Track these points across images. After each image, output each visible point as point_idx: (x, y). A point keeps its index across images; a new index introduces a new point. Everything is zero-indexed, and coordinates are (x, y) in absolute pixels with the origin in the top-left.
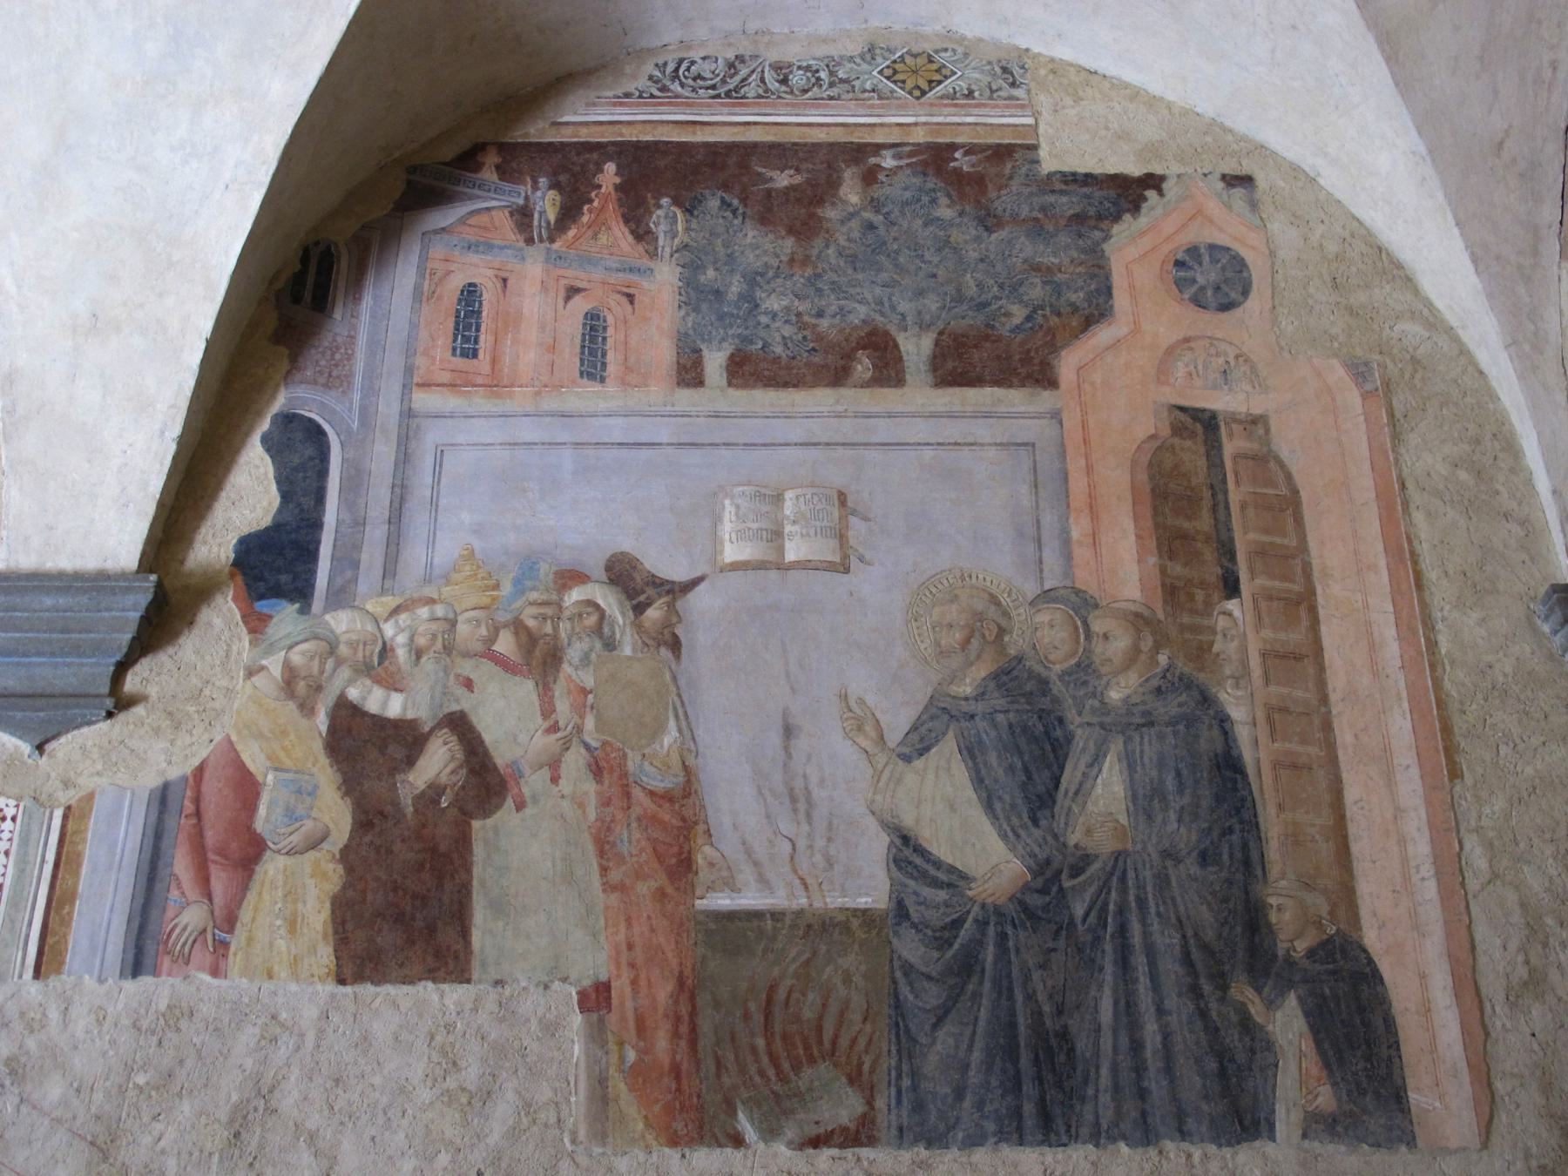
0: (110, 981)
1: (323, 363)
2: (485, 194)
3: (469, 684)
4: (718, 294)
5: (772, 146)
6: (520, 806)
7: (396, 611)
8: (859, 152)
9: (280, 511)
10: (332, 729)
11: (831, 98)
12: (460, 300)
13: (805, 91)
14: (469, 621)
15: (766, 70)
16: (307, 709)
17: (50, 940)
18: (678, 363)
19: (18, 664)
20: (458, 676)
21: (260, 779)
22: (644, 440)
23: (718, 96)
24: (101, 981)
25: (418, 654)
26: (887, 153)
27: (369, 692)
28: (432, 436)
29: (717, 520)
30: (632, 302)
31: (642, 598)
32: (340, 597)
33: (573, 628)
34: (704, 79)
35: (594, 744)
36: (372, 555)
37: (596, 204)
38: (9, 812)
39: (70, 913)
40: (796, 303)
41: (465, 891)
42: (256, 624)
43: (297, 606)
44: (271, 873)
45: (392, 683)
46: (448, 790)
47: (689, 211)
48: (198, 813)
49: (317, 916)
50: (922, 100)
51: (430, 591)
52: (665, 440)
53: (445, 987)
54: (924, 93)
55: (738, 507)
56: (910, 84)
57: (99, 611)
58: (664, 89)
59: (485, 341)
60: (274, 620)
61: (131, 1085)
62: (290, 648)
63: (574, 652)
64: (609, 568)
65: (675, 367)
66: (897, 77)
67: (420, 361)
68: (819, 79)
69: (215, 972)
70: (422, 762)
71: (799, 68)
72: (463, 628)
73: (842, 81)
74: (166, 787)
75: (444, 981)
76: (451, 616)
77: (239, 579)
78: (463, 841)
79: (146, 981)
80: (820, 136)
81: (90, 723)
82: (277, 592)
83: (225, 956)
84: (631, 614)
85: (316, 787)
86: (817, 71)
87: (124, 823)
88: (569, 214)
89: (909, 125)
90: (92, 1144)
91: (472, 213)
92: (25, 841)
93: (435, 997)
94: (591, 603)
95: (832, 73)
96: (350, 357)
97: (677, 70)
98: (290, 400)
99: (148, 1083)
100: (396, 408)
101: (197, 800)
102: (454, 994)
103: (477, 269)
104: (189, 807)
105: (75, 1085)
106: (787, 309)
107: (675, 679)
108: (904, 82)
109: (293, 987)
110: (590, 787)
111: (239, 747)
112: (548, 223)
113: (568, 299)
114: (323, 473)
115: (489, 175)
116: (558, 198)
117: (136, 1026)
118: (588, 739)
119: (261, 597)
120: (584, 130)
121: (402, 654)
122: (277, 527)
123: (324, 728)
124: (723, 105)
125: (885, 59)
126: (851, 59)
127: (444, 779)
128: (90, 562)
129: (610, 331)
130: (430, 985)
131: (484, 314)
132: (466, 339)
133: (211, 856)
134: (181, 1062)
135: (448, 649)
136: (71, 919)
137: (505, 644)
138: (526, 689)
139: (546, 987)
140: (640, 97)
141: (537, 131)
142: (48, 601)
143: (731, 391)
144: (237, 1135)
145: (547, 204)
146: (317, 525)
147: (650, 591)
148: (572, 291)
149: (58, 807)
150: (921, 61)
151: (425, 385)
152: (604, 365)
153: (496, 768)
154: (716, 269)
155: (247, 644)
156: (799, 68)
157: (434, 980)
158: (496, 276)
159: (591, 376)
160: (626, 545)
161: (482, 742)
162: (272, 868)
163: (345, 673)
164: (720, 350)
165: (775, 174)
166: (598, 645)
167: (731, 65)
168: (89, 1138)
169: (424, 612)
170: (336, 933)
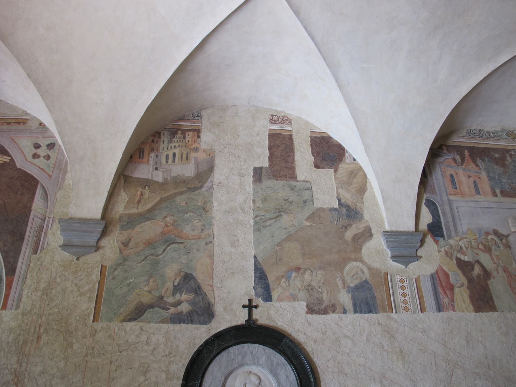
0: (435, 313)
1: (430, 189)
2: (446, 155)
3: (477, 254)
4: (494, 178)
5: (492, 148)
6: (494, 278)
7: (460, 240)
8: (508, 151)
9: (433, 219)
10: (457, 263)
11: (499, 139)
12: (450, 177)
13: (494, 138)
14: (474, 242)
15: (486, 132)
16: (451, 259)
17: (422, 305)
18: (492, 192)
19: (398, 250)
20: (475, 253)
21: (448, 273)
22: (491, 207)
23: (479, 138)
24: (434, 313)
25: (467, 248)
26: (512, 151)
27: (461, 256)
28: (455, 205)
29: (508, 223)
30: (480, 179)
31: (501, 238)
32: (450, 237)
33: (491, 244)
34: (476, 134)
35: (503, 266)
36: (452, 228)
37: (466, 158)
38: (405, 280)
39: (424, 300)
40: (508, 181)
41: (490, 294)
42: (437, 242)
43: (442, 238)
44: (457, 291)
45: (464, 254)
46: (481, 275)
47: (483, 161)
48: (440, 280)
49: (468, 300)
50: (514, 141)
51: (465, 236)
52: (494, 207)
53: (494, 313)
54: (514, 139)
55: (511, 221)
56: (511, 137)
57: (413, 239)
58: (470, 135)
59: (458, 186)
60: (440, 241)
61: (446, 333)
62: (444, 247)
63: (494, 248)
64: (494, 232)
65: (491, 193)
66: (509, 136)
67: (448, 190)
68: (495, 135)
69: (454, 311)
70: (475, 270)
71: (491, 133)
72: (473, 243)
73: (500, 136)
74: (432, 274)
75: (493, 312)
76: (470, 241)
77: (430, 233)
78: (487, 284)
79: (442, 313)
80: (499, 147)
81: (414, 262)
82: (437, 235)
83: (454, 307)
84: (500, 241)
85: (459, 274)
86: (494, 134)
87: (427, 282)
88: (463, 160)
89: (514, 146)
90: (443, 344)
91: (446, 159)
92: (410, 286)
93: (493, 315)
94: (493, 239)
95: (497, 134)
96: (435, 188)
97: (470, 131)
98: (427, 196)
99: (449, 332)
100: (446, 199)
101: (439, 277)
102: (496, 314)
103: (450, 171)
104: (438, 279)
105: (436, 333)
106: (507, 182)
107: (512, 254)
108: (510, 137)
109: (468, 313)
110: (504, 274)
111: (442, 267)
112: (460, 162)
113: (469, 178)
114: (438, 212)
115: (445, 151)
116: (460, 157)
117: (443, 321)
118: (501, 265)
119: (435, 237)
120: (459, 143)
121: (464, 248)
122: (433, 222)
123: (456, 263)
124: (481, 139)
125: (506, 132)
126: (499, 131)
127: (480, 273)
128: (406, 229)
129: (478, 185)
130: (491, 312)
131: (456, 180)
132: (454, 185)
133: (445, 288)
134: (453, 328)
135: (472, 247)
136: (424, 301)
137: (481, 246)
138: (487, 255)
139: (510, 312)
140: (466, 137)
141: (450, 142)
142: (403, 237)
143: (502, 198)
144: (468, 342)
145: (458, 158)
146: (440, 222)
147: (502, 237)
148: (469, 177)
149: (414, 279)
150: (511, 133)
151: (450, 194)
152: (479, 191)
153: (488, 271)
154: (492, 173)
155: (436, 247)
156: (491, 133)
157: (492, 312)
158: (455, 172)
159: (478, 194)
160: (495, 228)
161: (484, 266)
162: (457, 290)
163: (455, 252)
164: (498, 189)
165: (495, 154)
166: (497, 247)
167: (479, 131)
168: (442, 343)
169: (465, 240)
170: (472, 303)
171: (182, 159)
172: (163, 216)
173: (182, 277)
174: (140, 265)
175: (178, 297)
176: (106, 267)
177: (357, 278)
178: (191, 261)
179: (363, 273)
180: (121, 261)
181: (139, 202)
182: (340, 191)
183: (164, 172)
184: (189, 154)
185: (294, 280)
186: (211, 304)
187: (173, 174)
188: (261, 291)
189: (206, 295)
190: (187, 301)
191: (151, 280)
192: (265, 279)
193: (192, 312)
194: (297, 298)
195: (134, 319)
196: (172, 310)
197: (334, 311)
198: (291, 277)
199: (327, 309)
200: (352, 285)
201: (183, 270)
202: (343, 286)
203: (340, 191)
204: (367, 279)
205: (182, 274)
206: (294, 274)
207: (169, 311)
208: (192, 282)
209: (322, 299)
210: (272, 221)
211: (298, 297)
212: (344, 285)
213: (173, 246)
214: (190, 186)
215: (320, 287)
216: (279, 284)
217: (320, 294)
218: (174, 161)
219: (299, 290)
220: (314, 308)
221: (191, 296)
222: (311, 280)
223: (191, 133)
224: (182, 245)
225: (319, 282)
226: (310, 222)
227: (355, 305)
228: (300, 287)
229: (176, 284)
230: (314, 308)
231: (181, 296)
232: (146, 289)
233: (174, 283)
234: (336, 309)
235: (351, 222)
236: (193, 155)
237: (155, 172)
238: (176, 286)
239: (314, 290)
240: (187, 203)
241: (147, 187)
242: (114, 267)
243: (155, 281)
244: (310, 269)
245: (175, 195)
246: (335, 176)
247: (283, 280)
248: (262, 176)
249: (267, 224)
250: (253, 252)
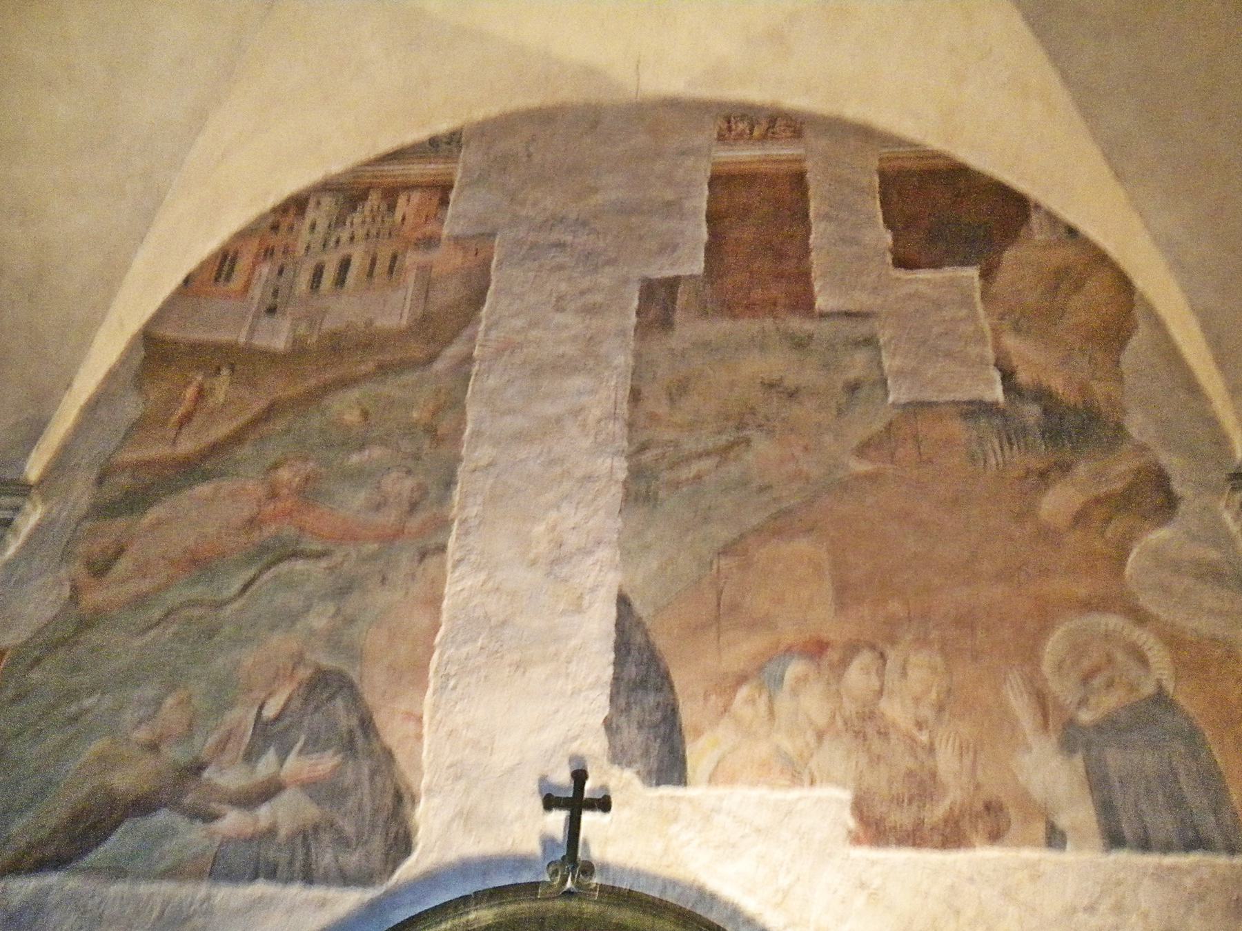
171: (370, 274)
172: (268, 463)
173: (300, 685)
174: (137, 643)
175: (266, 765)
177: (1110, 685)
178: (350, 621)
179: (1143, 661)
181: (187, 418)
182: (1011, 342)
183: (296, 322)
184: (400, 257)
187: (328, 325)
188: (639, 739)
191: (170, 701)
193: (316, 828)
194: (807, 771)
195: (58, 863)
196: (233, 821)
197: (995, 836)
202: (1039, 718)
203: (1011, 342)
204: (1160, 687)
205: (304, 673)
206: (796, 669)
209: (934, 775)
210: (707, 464)
212: (1045, 716)
213: (284, 567)
214: (387, 357)
215: (920, 725)
216: (726, 709)
217: (922, 755)
218: (340, 280)
219: (820, 736)
222: (880, 692)
223: (416, 196)
224: (323, 563)
226: (872, 461)
227: (1106, 809)
228: (821, 720)
229: (270, 712)
230: (892, 818)
231: (282, 761)
232: (142, 734)
233: (261, 707)
235: (1068, 457)
236: (412, 259)
237: (265, 321)
239: (893, 737)
240: (365, 414)
241: (225, 372)
242: (37, 653)
243: (185, 703)
244: (873, 647)
245: (326, 389)
246: (984, 294)
248: (674, 310)
249: (687, 473)
250: (612, 581)
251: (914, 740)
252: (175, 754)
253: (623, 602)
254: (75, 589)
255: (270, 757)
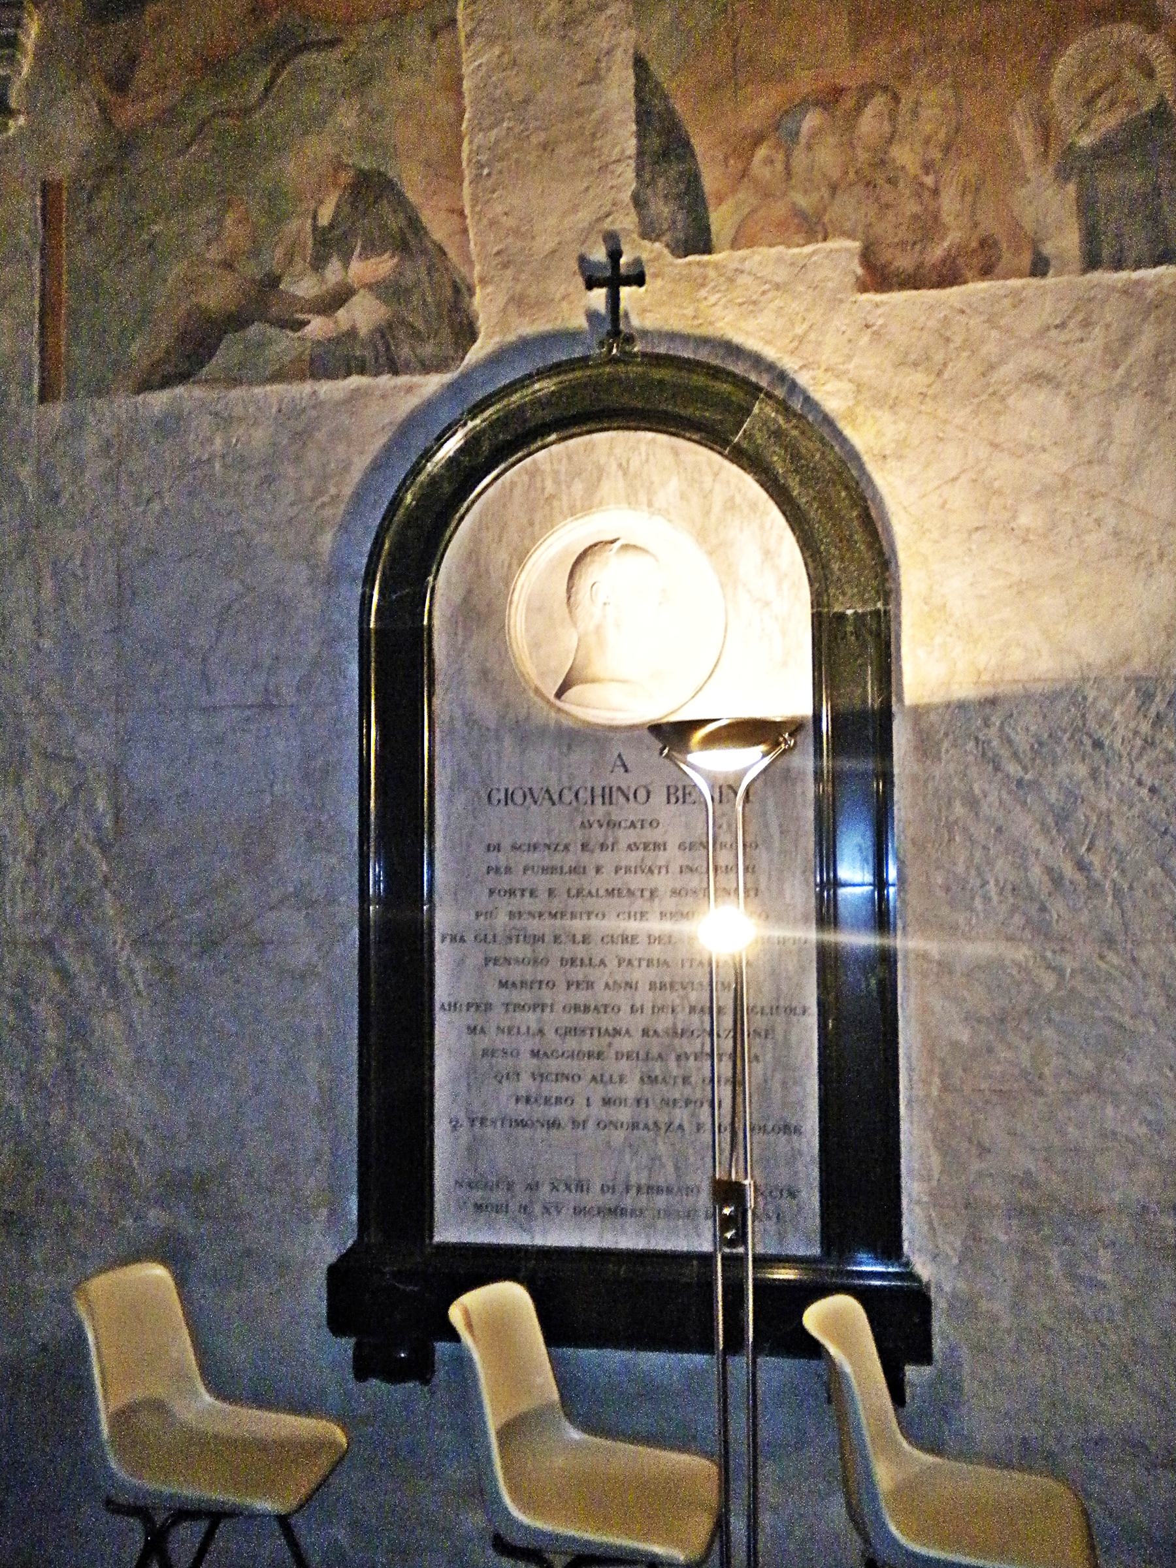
175: (333, 272)
176: (59, 187)
179: (1150, 74)
180: (111, 156)
185: (809, 147)
186: (464, 290)
189: (445, 254)
190: (369, 287)
192: (681, 159)
193: (390, 325)
195: (183, 377)
196: (317, 326)
197: (986, 272)
198: (797, 133)
199: (953, 262)
200: (1085, 141)
201: (346, 159)
205: (345, 177)
206: (812, 120)
207: (308, 328)
208: (385, 207)
211: (826, 219)
216: (744, 173)
219: (834, 189)
220: (896, 264)
221: (383, 266)
224: (338, 53)
225: (927, 141)
227: (1091, 235)
228: (835, 174)
229: (324, 220)
230: (896, 264)
231: (346, 266)
232: (214, 254)
233: (315, 218)
234: (999, 258)
238: (324, 228)
244: (885, 89)
247: (762, 152)
251: (922, 184)
252: (252, 270)
253: (640, 64)
254: (103, 108)
255: (335, 265)
